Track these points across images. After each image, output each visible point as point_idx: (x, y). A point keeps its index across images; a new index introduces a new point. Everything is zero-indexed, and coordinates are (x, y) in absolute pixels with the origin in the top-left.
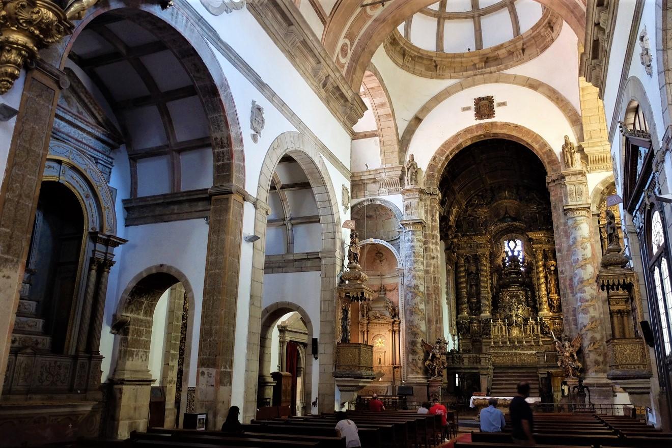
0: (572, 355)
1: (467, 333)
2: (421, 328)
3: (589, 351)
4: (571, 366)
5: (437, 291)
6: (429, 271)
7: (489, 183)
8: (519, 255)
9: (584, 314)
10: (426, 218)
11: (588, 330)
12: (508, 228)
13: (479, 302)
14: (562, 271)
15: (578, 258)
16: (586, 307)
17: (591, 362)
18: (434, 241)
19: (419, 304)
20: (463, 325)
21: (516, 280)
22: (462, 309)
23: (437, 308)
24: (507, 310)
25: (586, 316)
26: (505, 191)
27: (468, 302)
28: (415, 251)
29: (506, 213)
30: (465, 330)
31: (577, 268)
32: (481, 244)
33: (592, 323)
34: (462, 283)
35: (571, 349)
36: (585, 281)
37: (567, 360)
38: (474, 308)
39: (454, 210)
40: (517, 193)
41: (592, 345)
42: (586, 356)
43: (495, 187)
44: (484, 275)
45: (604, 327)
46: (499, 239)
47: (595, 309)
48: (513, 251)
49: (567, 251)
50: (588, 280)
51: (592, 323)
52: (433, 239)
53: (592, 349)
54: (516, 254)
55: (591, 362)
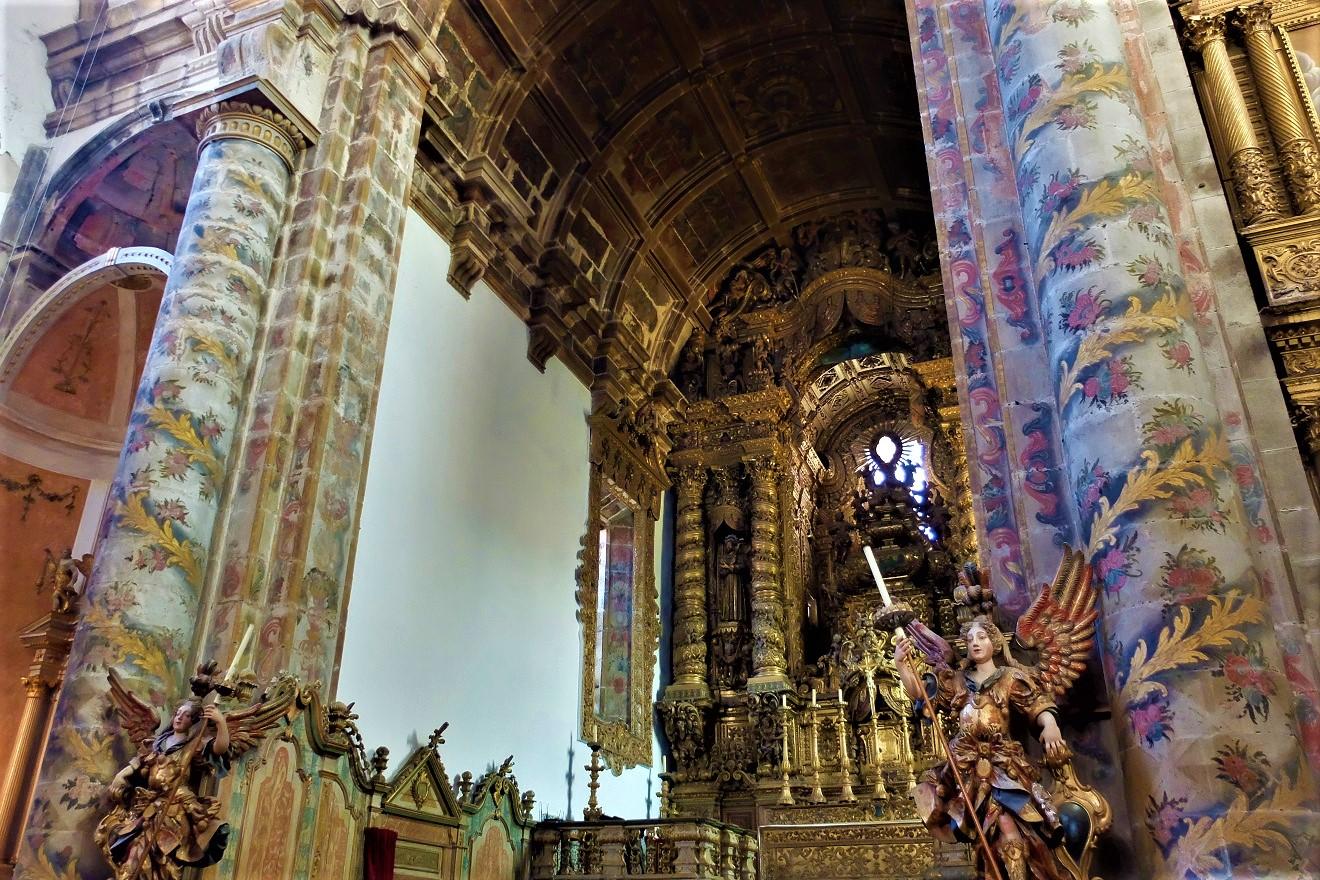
0: (1023, 726)
1: (699, 754)
2: (130, 613)
3: (1156, 677)
4: (1015, 817)
5: (310, 432)
6: (286, 335)
7: (779, 210)
8: (910, 480)
9: (1100, 400)
10: (325, 113)
11: (1142, 510)
12: (877, 405)
13: (746, 636)
14: (960, 222)
15: (1035, 81)
16: (1114, 348)
17: (1189, 771)
18: (347, 209)
19: (156, 476)
20: (681, 724)
21: (895, 558)
22: (684, 662)
23: (293, 517)
24: (849, 659)
25: (1116, 408)
26: (839, 240)
27: (708, 638)
28: (205, 224)
29: (846, 318)
30: (690, 744)
31: (1034, 134)
32: (758, 423)
33: (1167, 452)
34: (686, 566)
35: (1017, 672)
36: (1093, 185)
37: (984, 767)
38: (730, 659)
39: (662, 311)
40: (882, 248)
41: (1181, 624)
42: (1143, 721)
43: (806, 236)
44: (767, 532)
45: (1264, 514)
46: (849, 443)
47: (1181, 358)
48: (888, 469)
49: (980, 106)
50: (1112, 179)
51: (1167, 452)
52: (345, 199)
53: (1187, 656)
54: (900, 475)
55: (1189, 771)
